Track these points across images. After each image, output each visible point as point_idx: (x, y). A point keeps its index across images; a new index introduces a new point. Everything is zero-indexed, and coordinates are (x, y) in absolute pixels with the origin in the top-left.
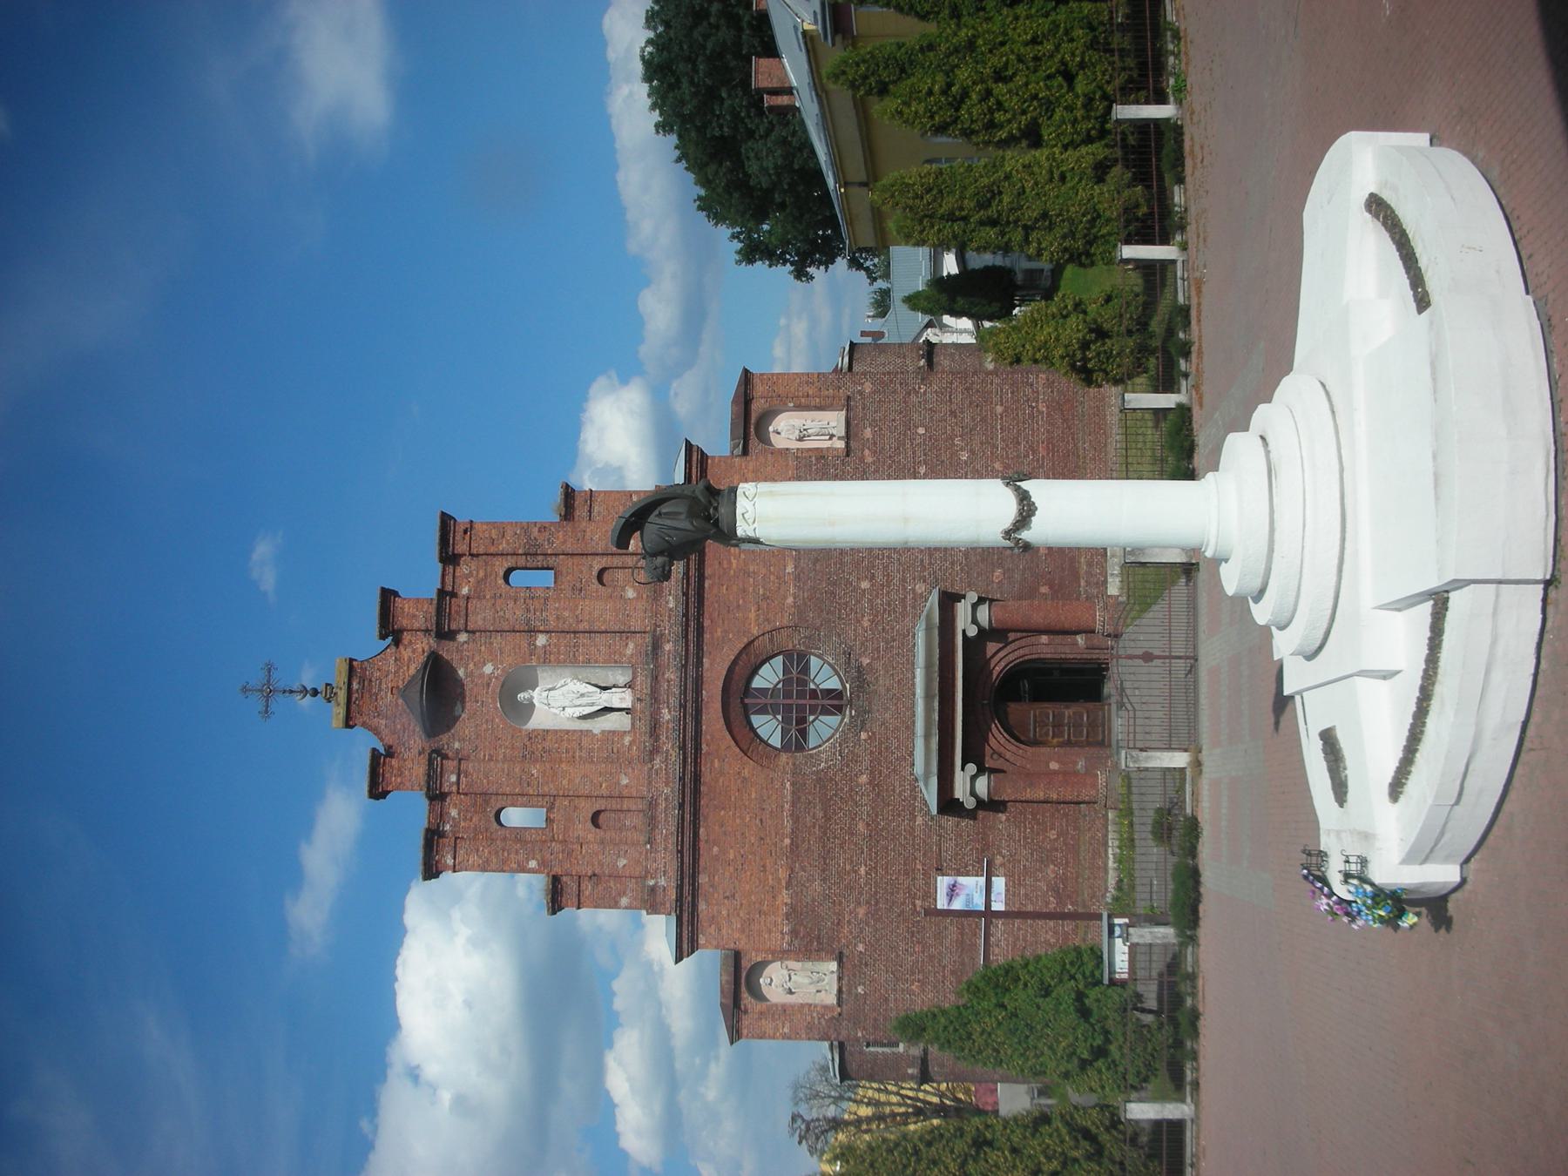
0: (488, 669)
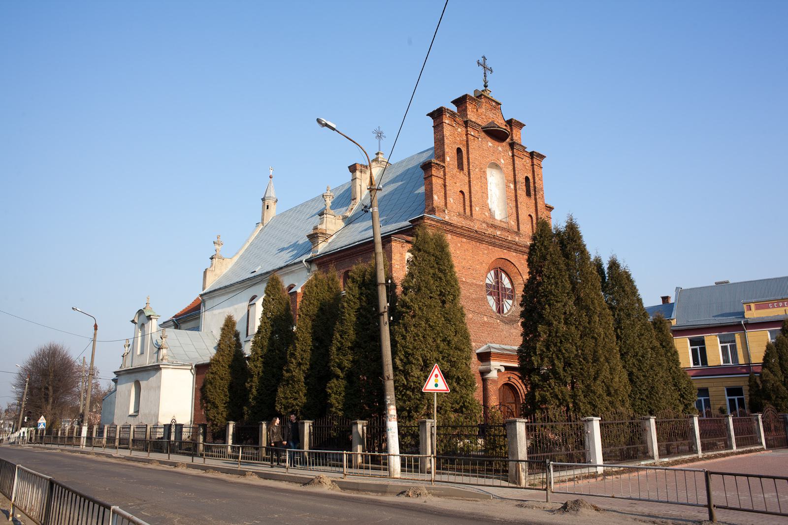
0: (502, 161)
